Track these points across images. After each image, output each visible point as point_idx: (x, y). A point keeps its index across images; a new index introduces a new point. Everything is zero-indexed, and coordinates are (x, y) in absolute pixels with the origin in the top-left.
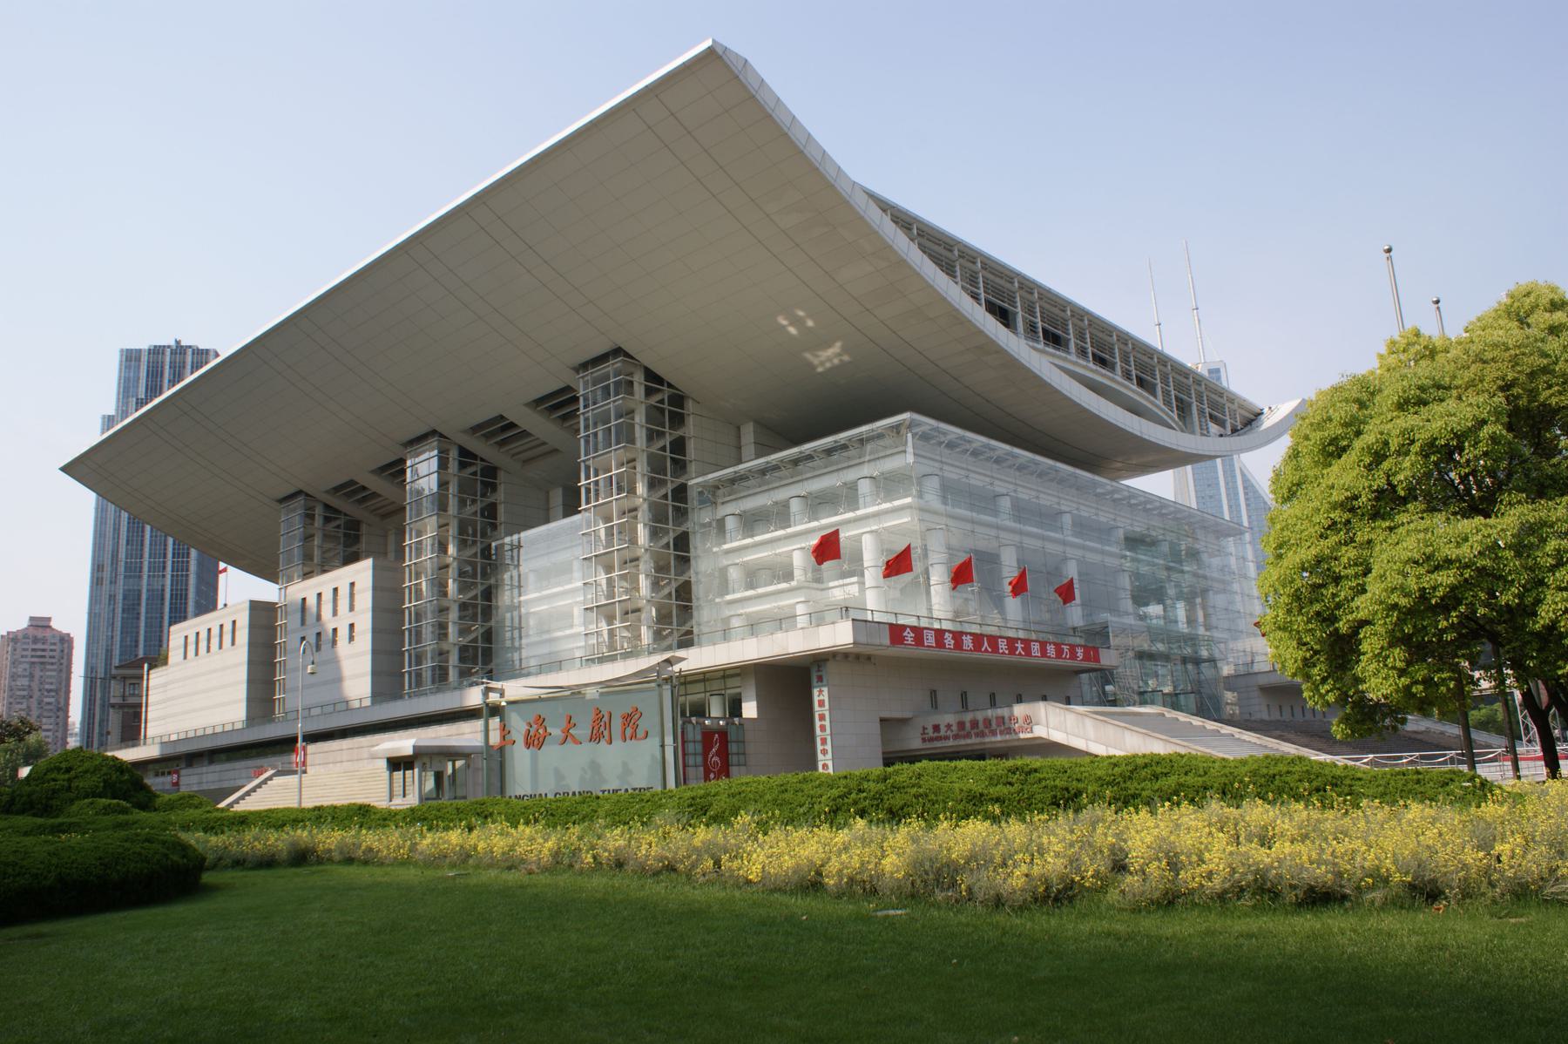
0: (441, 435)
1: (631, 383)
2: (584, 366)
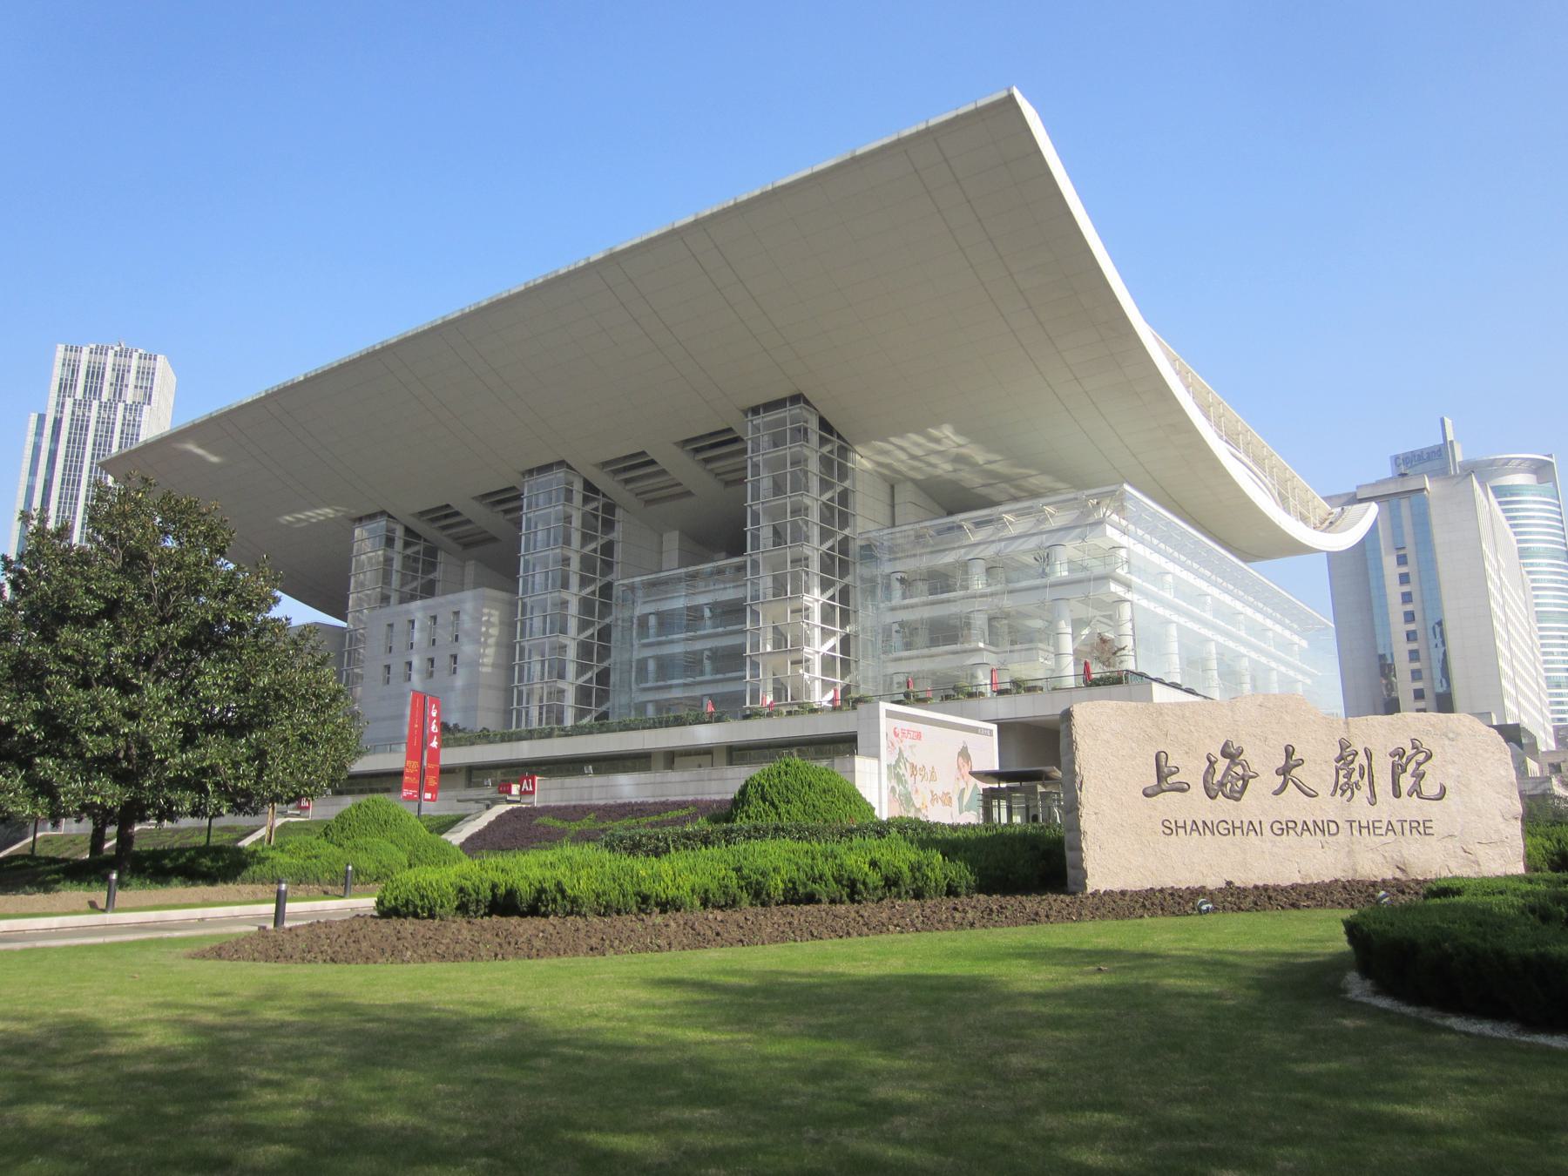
2: (755, 410)
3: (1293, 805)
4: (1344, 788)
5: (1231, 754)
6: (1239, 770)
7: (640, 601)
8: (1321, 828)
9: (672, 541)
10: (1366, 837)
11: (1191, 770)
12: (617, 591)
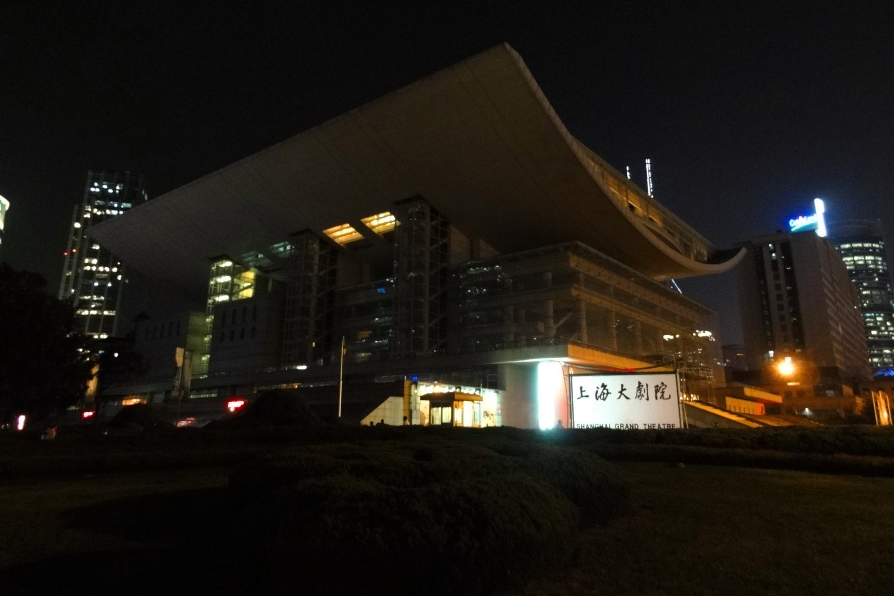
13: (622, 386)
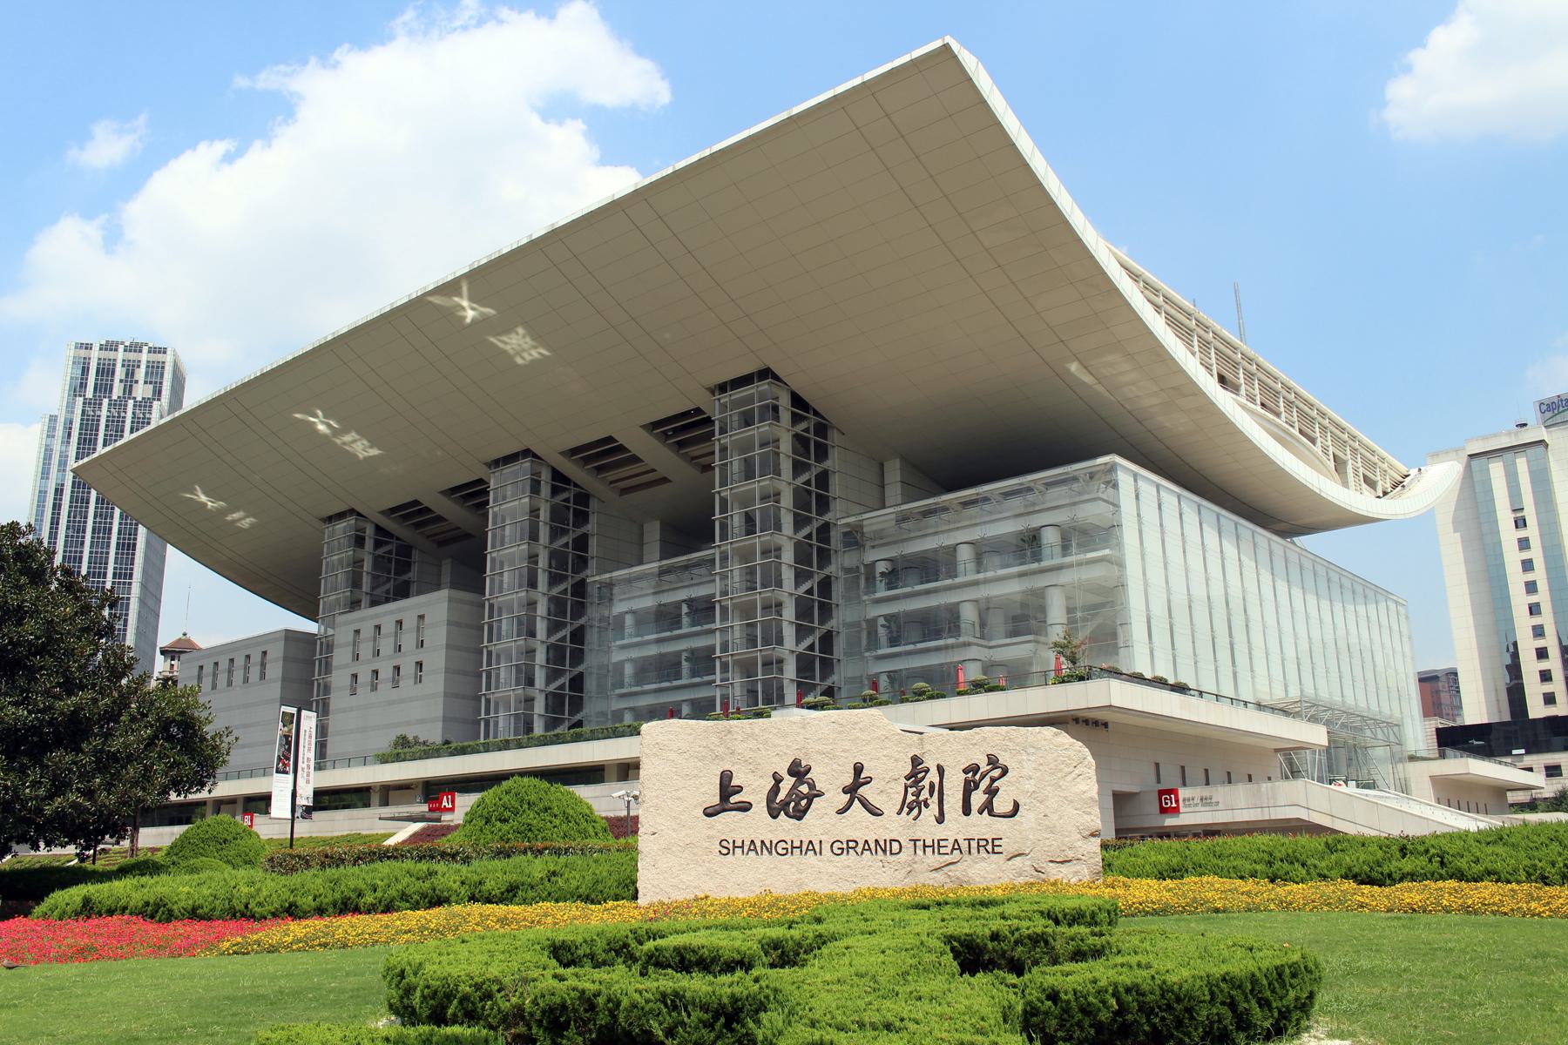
0: (535, 456)
1: (776, 409)
2: (722, 388)
3: (858, 824)
4: (913, 806)
5: (798, 771)
6: (804, 789)
7: (616, 598)
8: (884, 847)
9: (653, 532)
10: (932, 859)
11: (755, 789)
12: (592, 591)
13: (858, 769)
